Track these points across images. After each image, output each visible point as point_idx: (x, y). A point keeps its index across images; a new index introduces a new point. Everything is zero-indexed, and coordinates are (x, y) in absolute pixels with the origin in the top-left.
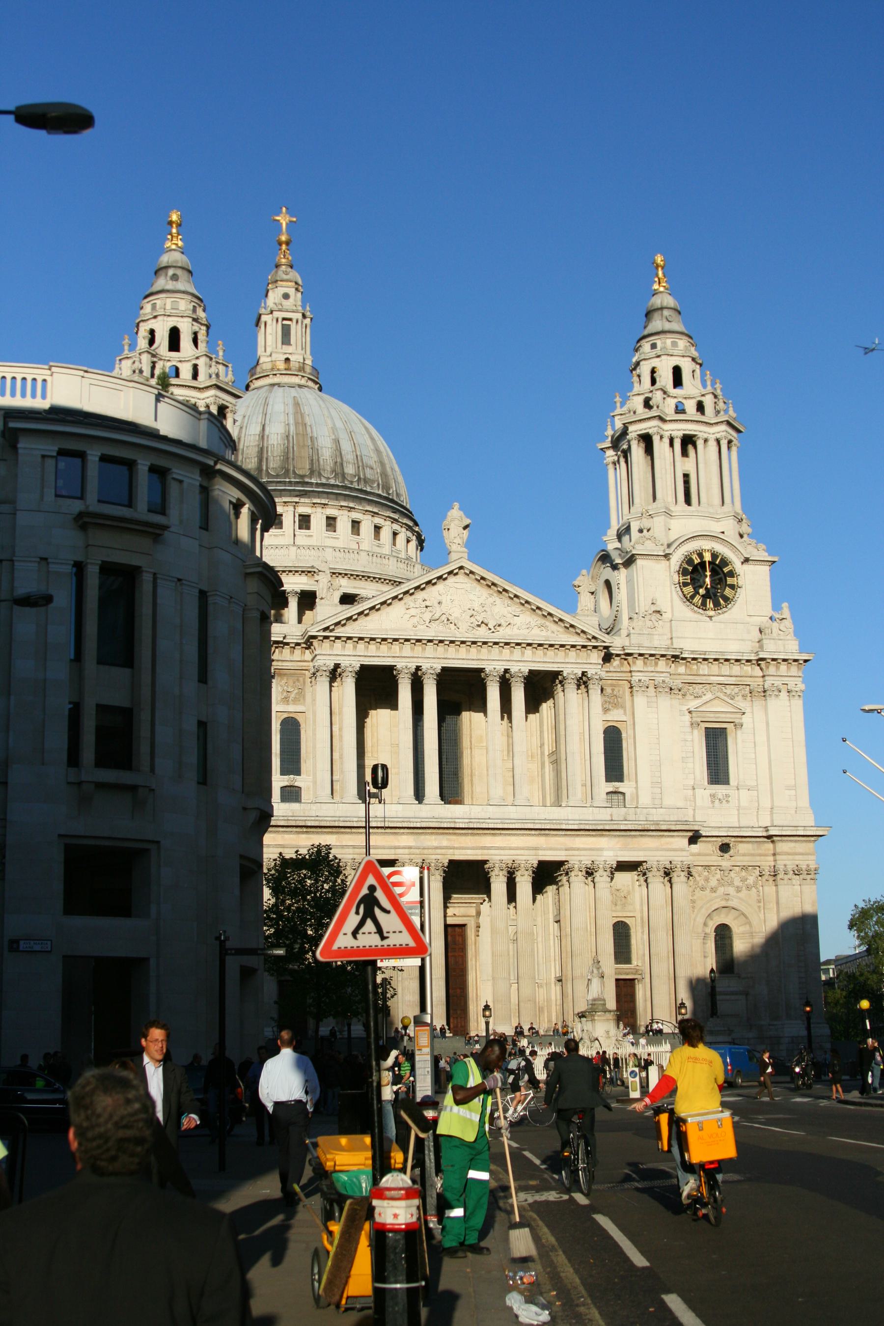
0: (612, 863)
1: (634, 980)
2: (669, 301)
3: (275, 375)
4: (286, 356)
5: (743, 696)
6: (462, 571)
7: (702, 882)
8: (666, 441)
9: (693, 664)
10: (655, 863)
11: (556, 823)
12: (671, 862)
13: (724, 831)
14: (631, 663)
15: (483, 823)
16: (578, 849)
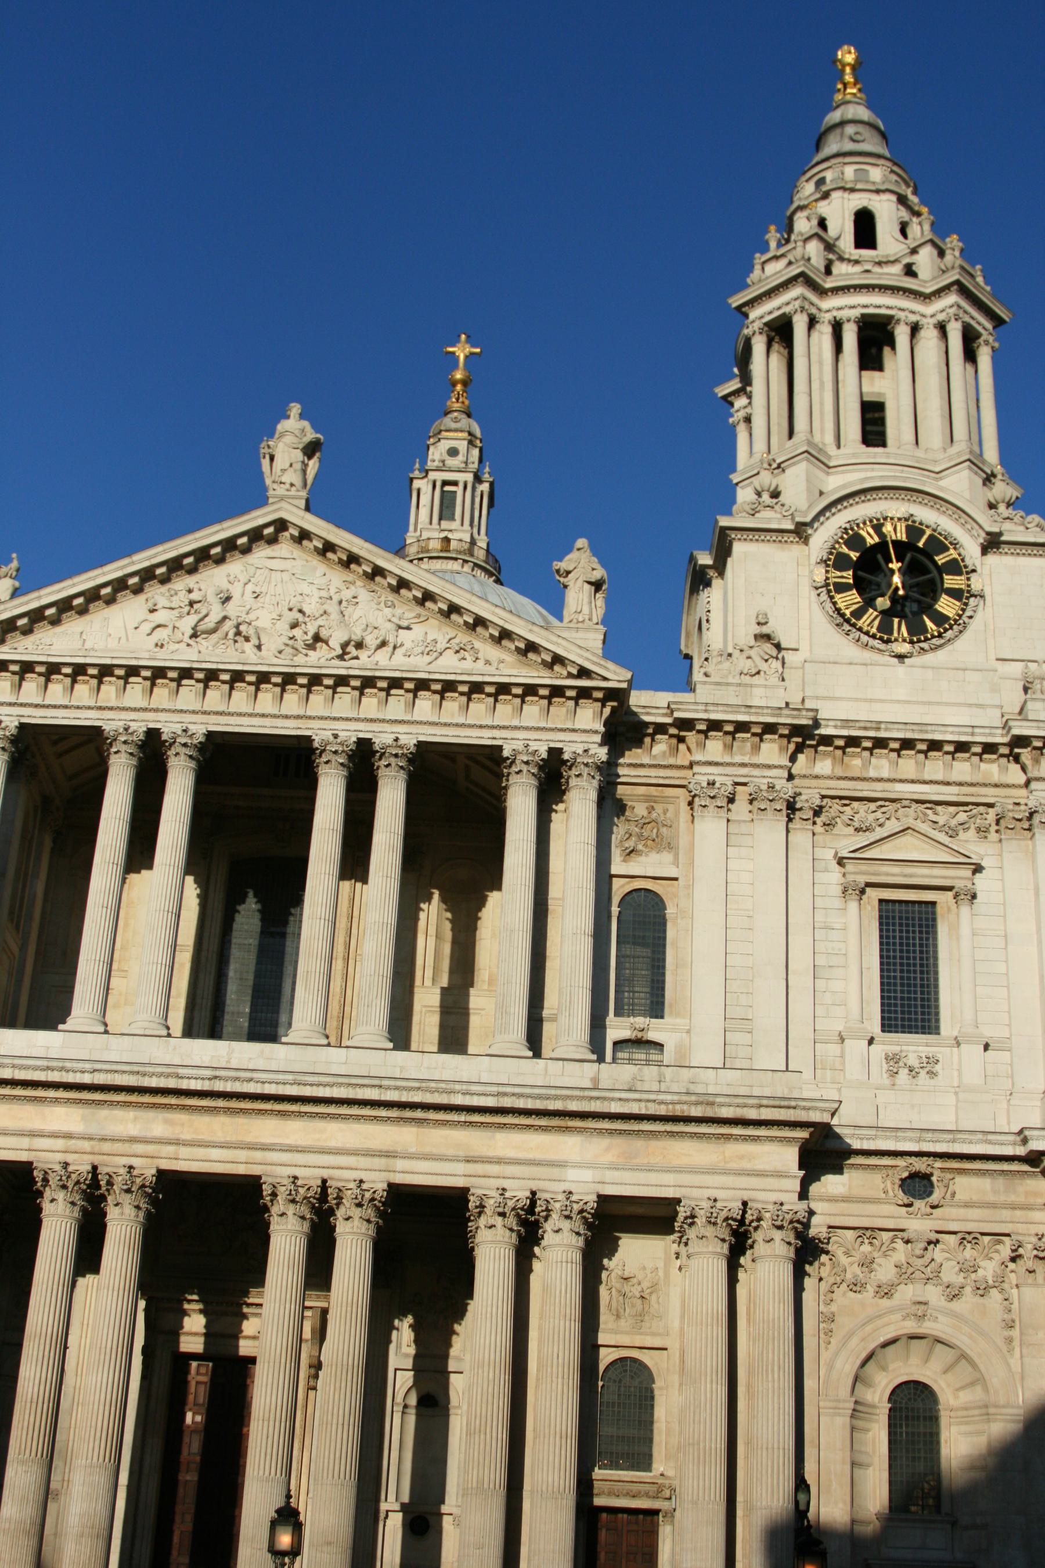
0: (586, 1198)
1: (655, 1512)
2: (863, 113)
3: (421, 559)
4: (443, 535)
5: (979, 830)
6: (286, 534)
7: (854, 1271)
8: (824, 331)
9: (854, 755)
10: (706, 1205)
11: (437, 1091)
12: (745, 1204)
13: (911, 1140)
14: (693, 746)
15: (251, 1080)
16: (499, 1161)
